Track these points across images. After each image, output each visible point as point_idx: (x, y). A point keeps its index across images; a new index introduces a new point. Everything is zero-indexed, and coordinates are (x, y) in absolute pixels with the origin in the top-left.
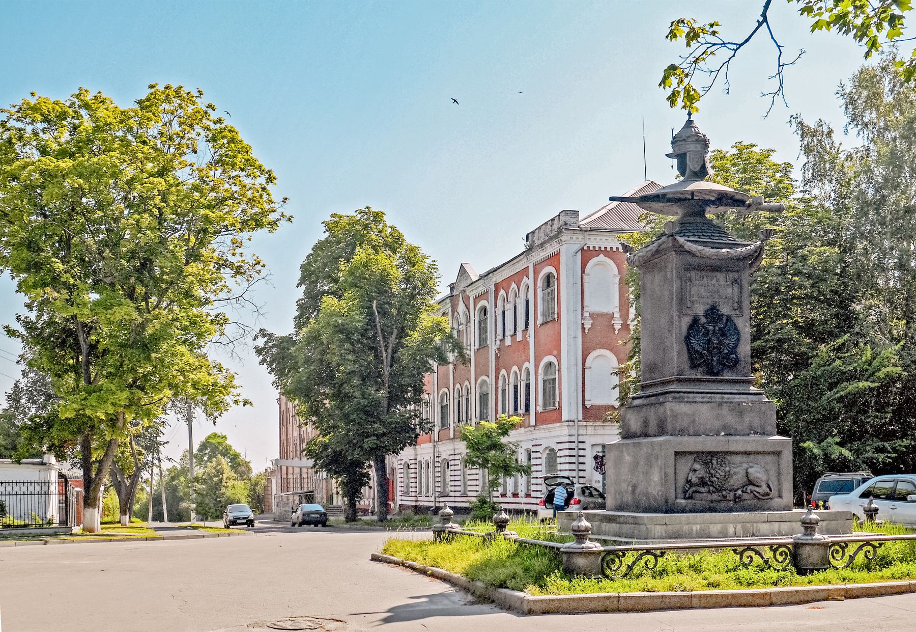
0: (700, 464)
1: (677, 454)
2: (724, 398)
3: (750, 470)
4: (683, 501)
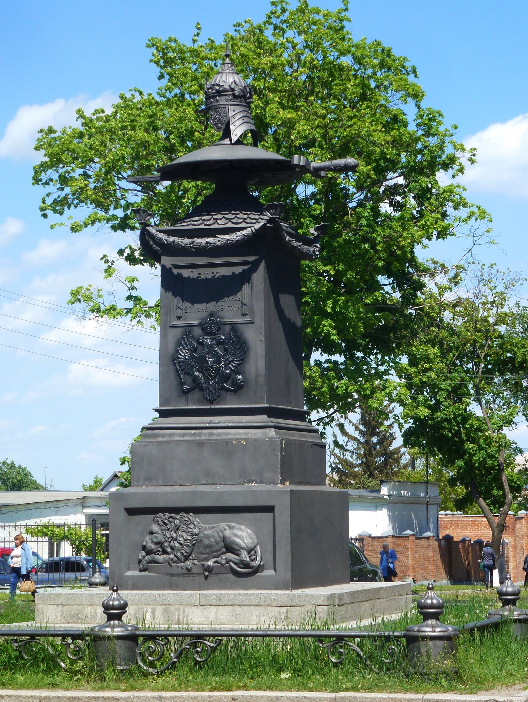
0: (159, 524)
1: (131, 512)
2: (212, 434)
3: (227, 533)
4: (136, 573)
